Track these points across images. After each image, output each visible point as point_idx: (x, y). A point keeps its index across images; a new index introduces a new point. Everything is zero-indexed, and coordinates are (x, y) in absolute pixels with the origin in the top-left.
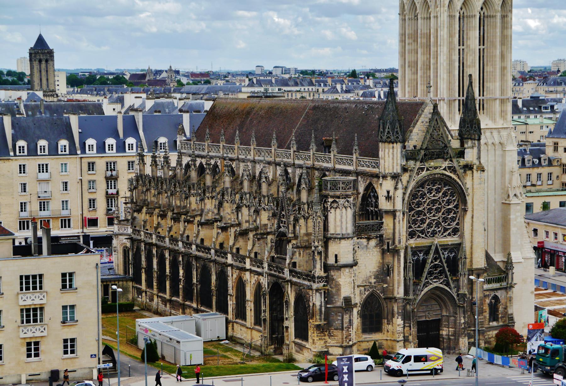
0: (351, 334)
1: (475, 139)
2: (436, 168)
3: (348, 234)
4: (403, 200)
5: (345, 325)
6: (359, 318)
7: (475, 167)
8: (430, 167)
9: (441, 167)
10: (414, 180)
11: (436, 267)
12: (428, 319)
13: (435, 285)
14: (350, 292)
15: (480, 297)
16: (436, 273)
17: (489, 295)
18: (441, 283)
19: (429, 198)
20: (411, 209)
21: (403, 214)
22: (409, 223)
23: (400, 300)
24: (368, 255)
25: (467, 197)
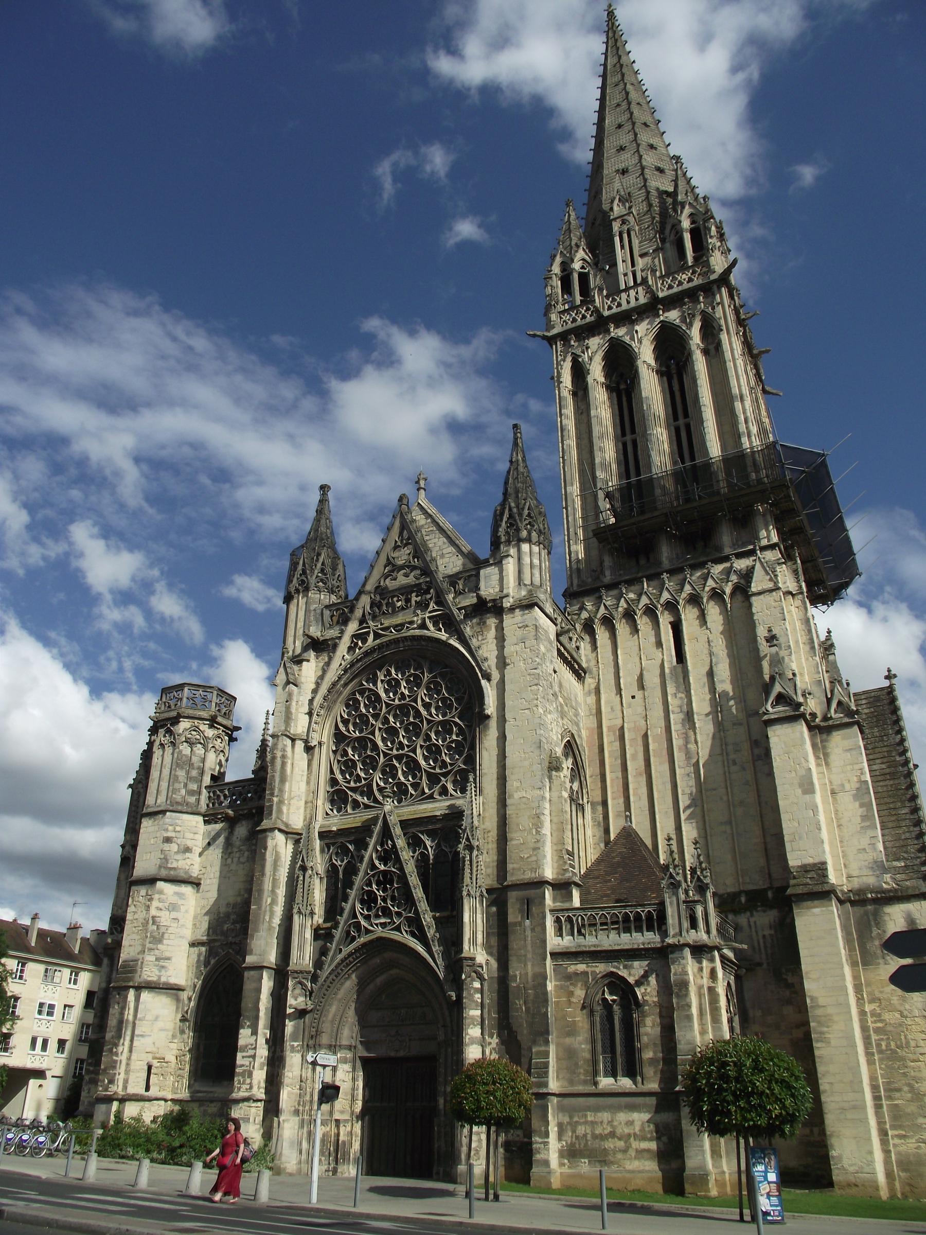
0: (116, 1062)
1: (508, 542)
2: (399, 627)
3: (159, 806)
4: (310, 714)
5: (108, 1036)
6: (187, 1031)
7: (507, 604)
8: (382, 629)
9: (411, 623)
10: (341, 665)
11: (385, 880)
12: (392, 1054)
13: (379, 932)
14: (139, 948)
15: (535, 976)
16: (384, 900)
17: (585, 973)
18: (398, 929)
19: (388, 705)
20: (339, 737)
21: (309, 749)
22: (332, 772)
23: (252, 973)
24: (229, 861)
25: (484, 683)
